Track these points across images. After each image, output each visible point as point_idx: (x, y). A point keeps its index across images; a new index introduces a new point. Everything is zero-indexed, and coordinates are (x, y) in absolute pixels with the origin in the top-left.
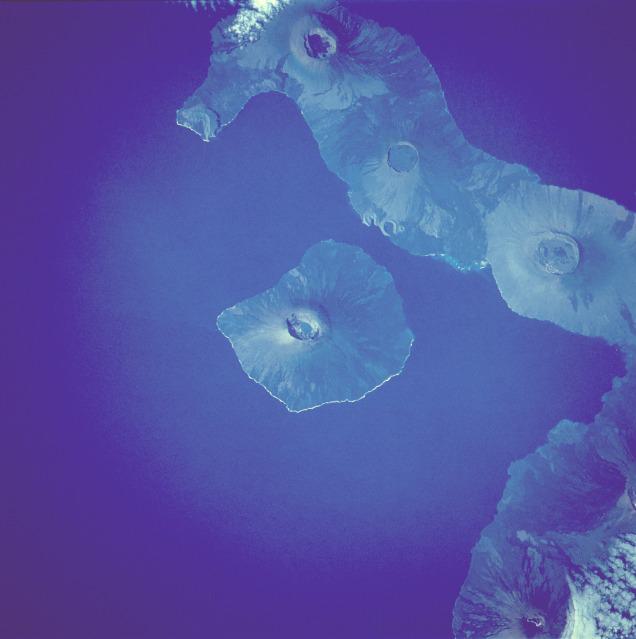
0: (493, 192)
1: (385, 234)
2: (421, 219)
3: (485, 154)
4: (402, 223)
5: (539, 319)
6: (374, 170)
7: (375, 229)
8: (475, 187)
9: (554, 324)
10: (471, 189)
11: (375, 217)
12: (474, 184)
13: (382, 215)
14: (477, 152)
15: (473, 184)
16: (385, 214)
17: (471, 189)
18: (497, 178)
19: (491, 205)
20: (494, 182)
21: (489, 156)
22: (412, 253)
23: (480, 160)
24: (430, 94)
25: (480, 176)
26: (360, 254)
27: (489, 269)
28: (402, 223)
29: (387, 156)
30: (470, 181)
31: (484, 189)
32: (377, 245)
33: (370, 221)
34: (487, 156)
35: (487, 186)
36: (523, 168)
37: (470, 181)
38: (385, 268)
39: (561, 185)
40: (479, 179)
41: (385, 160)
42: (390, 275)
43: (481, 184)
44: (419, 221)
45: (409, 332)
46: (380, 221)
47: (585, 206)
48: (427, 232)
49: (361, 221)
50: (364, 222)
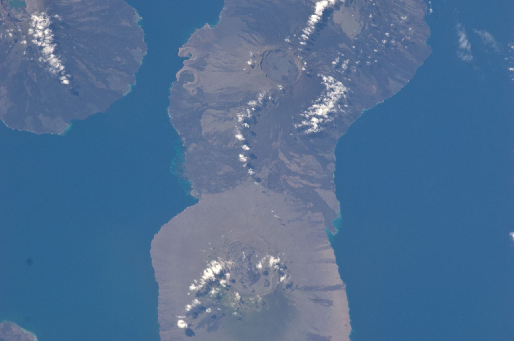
0: (288, 182)
1: (178, 75)
2: (217, 108)
3: (333, 165)
4: (200, 90)
5: (157, 275)
6: (250, 42)
7: (179, 63)
8: (287, 161)
9: (158, 295)
10: (282, 156)
11: (194, 58)
12: (290, 160)
13: (200, 65)
14: (331, 155)
15: (290, 158)
16: (202, 69)
17: (282, 156)
18: (311, 185)
19: (273, 183)
20: (305, 182)
21: (333, 169)
22: (169, 110)
23: (324, 162)
24: (374, 87)
25: (303, 164)
26: (139, 54)
27: (193, 201)
28: (200, 90)
29: (273, 48)
30: (291, 153)
31: (290, 173)
32: (161, 68)
33: (185, 55)
34: (332, 167)
35: (295, 174)
36: (338, 212)
37: (291, 153)
38: (135, 83)
39: (339, 261)
40: (299, 164)
41: (267, 48)
42: (130, 90)
43: (294, 168)
44: (213, 108)
45: (68, 126)
46: (189, 66)
47: (327, 295)
48: (202, 121)
49: (181, 47)
50: (181, 50)
